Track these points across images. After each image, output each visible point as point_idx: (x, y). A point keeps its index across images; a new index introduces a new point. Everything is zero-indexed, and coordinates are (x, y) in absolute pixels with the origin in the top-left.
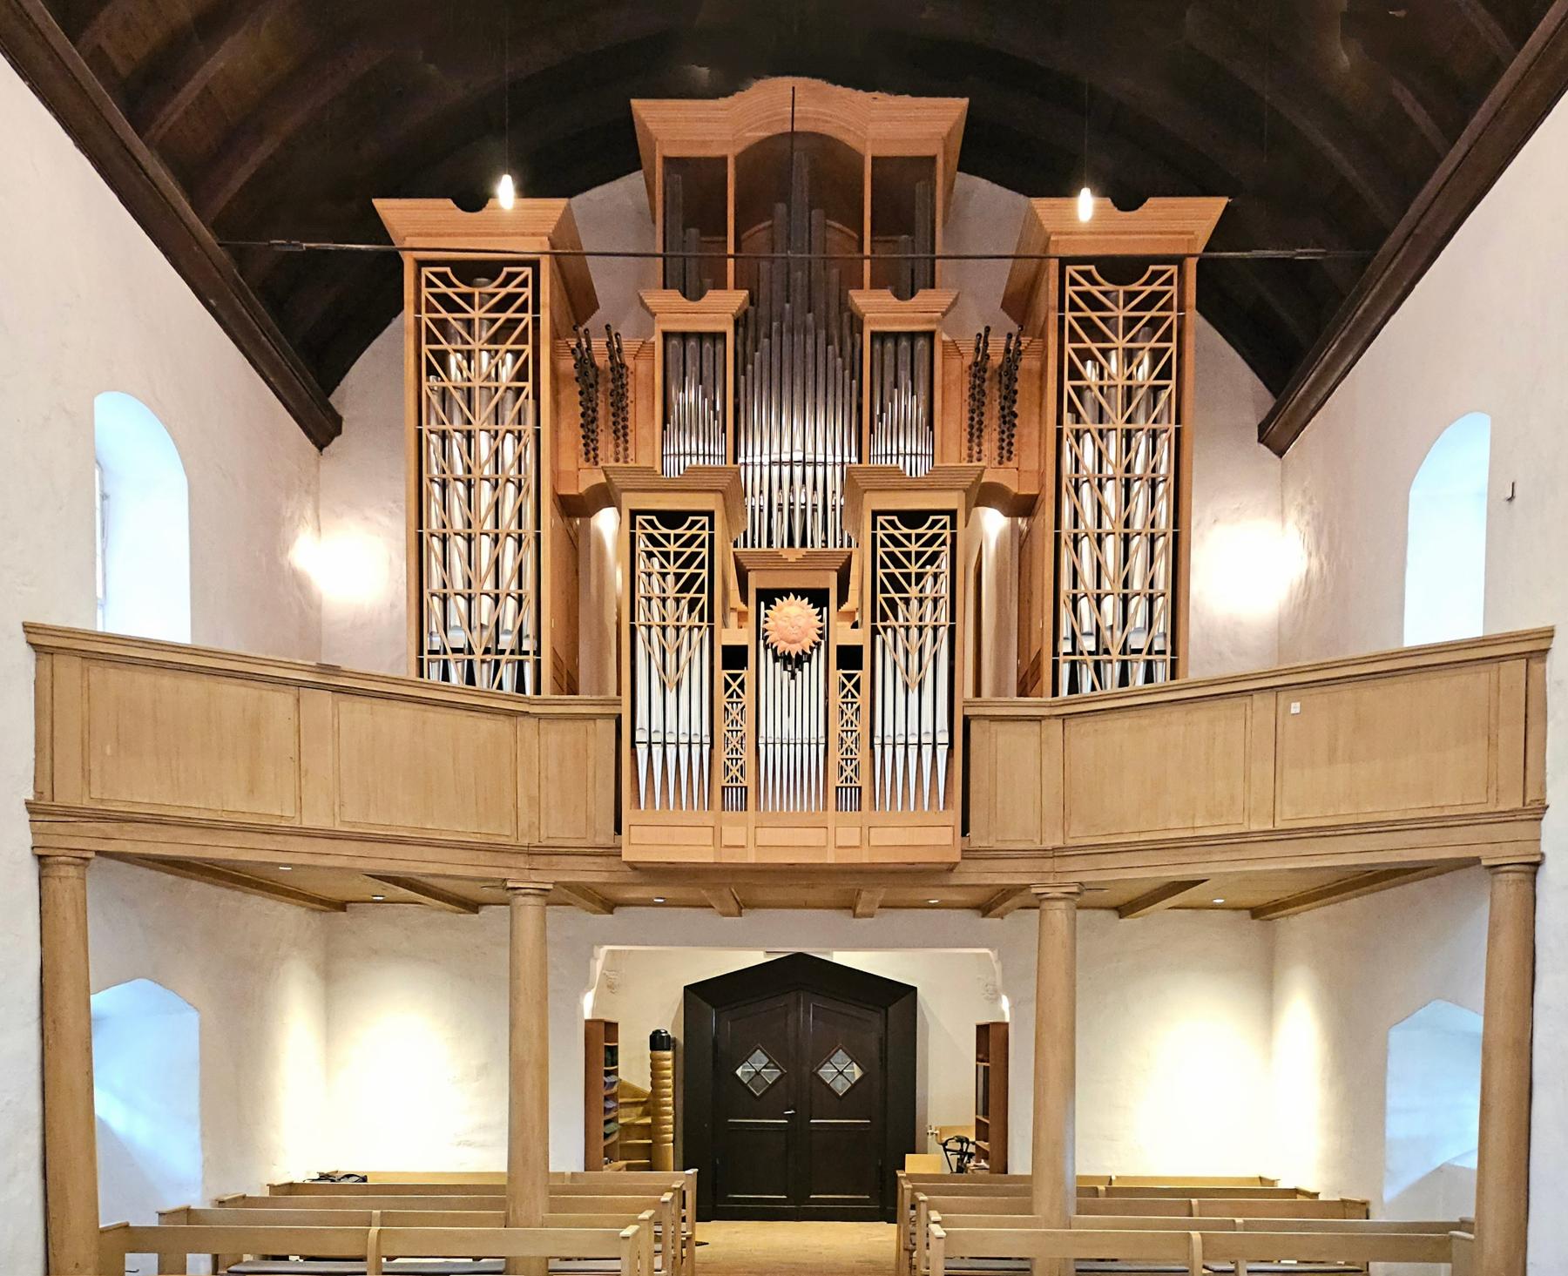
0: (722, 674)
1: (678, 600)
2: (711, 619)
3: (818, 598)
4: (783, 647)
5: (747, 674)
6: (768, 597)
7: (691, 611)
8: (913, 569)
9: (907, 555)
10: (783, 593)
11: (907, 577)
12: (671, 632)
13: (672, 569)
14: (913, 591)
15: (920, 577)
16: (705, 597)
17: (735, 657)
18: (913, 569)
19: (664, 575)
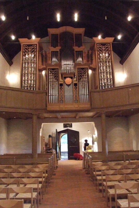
0: (60, 87)
1: (54, 79)
2: (58, 80)
3: (72, 78)
4: (67, 83)
5: (63, 87)
6: (65, 78)
7: (56, 79)
8: (83, 74)
9: (82, 73)
10: (68, 77)
11: (82, 75)
12: (53, 82)
13: (53, 75)
14: (83, 77)
15: (84, 75)
16: (57, 78)
17: (61, 85)
18: (83, 74)
19: (52, 76)
